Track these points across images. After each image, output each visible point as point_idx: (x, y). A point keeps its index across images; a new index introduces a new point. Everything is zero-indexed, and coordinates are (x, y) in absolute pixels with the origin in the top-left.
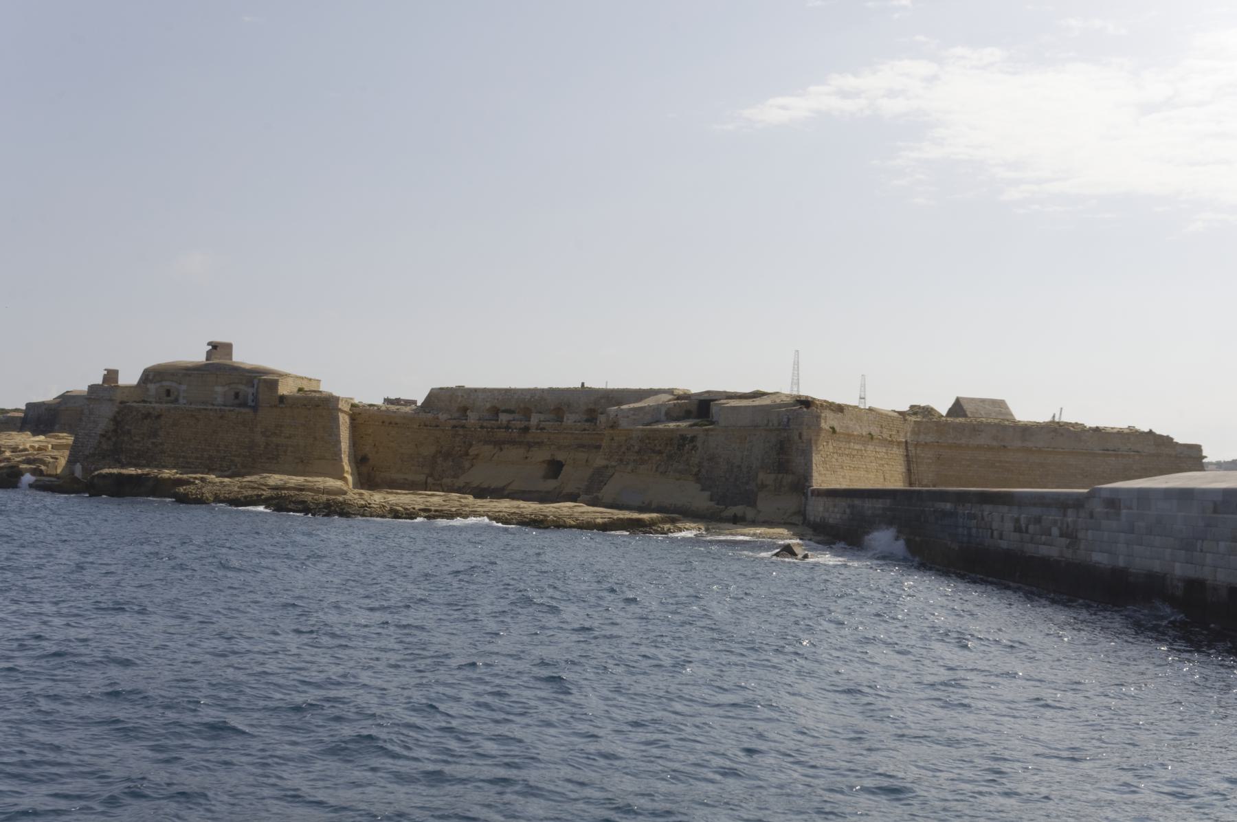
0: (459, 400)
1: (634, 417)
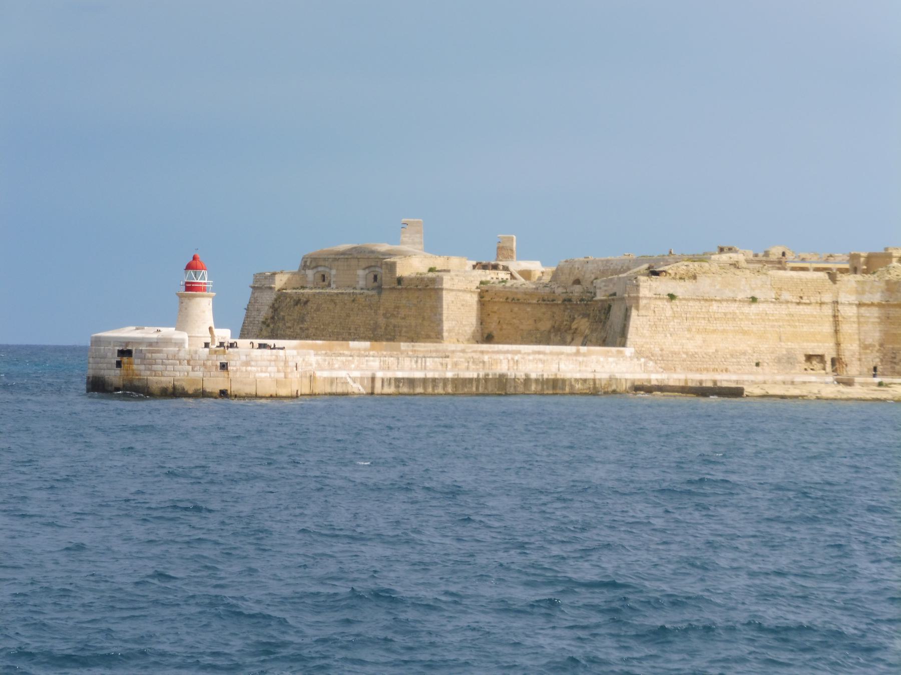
0: (577, 271)
1: (606, 288)
